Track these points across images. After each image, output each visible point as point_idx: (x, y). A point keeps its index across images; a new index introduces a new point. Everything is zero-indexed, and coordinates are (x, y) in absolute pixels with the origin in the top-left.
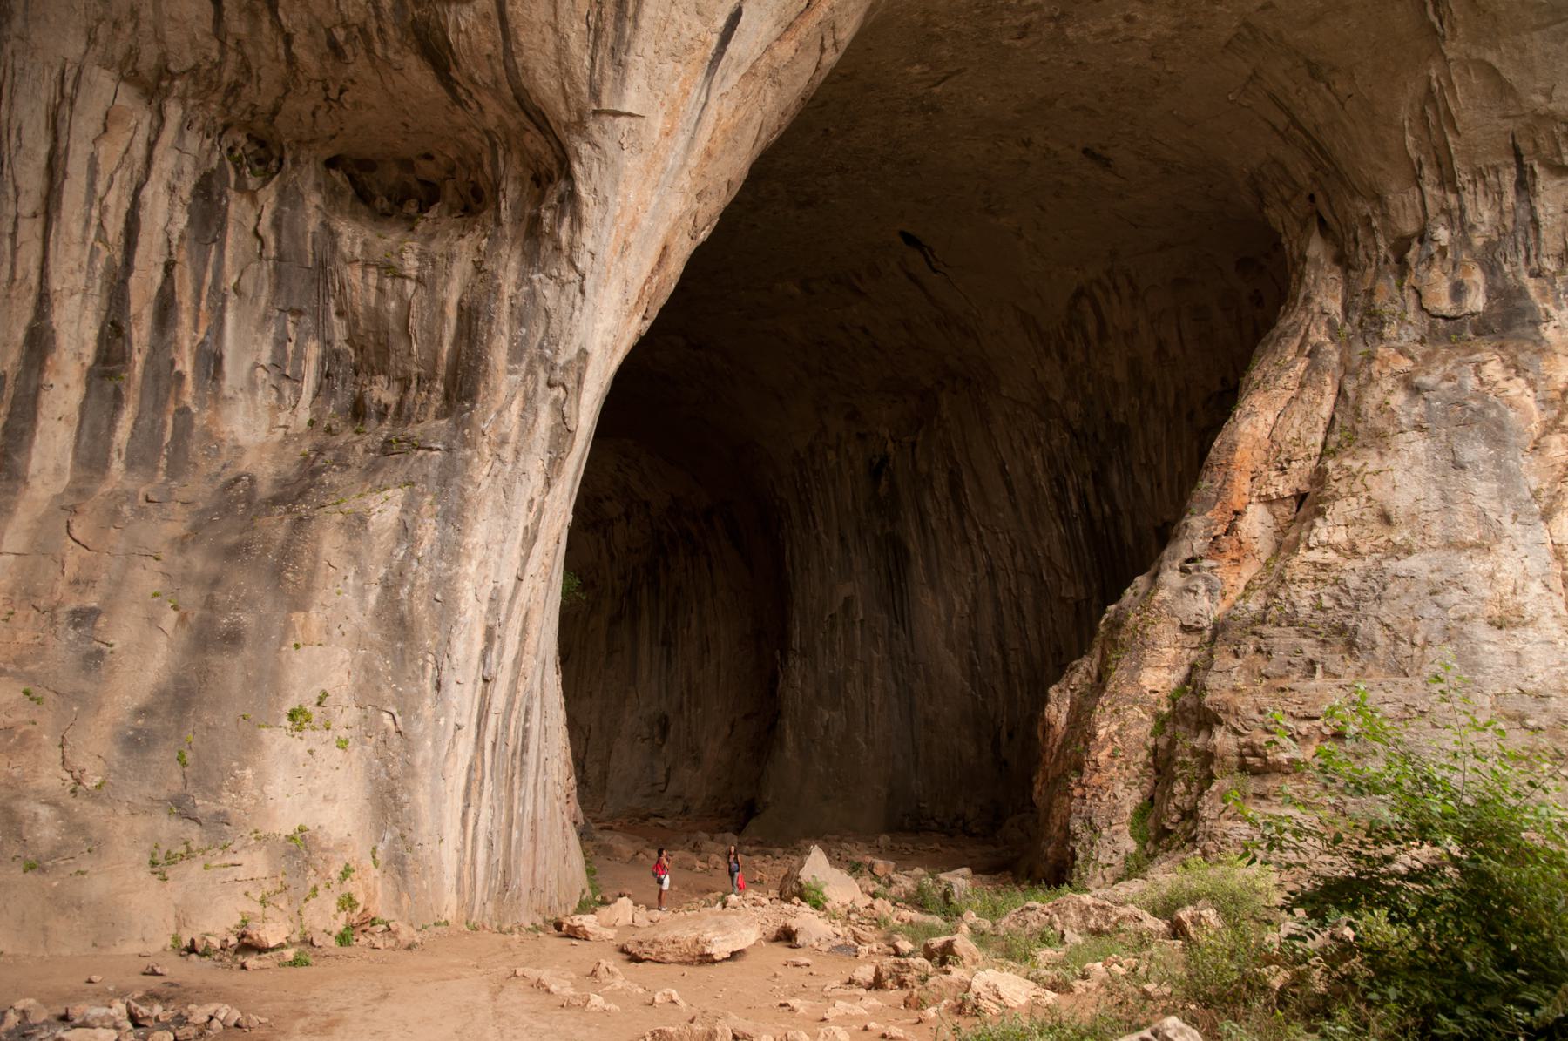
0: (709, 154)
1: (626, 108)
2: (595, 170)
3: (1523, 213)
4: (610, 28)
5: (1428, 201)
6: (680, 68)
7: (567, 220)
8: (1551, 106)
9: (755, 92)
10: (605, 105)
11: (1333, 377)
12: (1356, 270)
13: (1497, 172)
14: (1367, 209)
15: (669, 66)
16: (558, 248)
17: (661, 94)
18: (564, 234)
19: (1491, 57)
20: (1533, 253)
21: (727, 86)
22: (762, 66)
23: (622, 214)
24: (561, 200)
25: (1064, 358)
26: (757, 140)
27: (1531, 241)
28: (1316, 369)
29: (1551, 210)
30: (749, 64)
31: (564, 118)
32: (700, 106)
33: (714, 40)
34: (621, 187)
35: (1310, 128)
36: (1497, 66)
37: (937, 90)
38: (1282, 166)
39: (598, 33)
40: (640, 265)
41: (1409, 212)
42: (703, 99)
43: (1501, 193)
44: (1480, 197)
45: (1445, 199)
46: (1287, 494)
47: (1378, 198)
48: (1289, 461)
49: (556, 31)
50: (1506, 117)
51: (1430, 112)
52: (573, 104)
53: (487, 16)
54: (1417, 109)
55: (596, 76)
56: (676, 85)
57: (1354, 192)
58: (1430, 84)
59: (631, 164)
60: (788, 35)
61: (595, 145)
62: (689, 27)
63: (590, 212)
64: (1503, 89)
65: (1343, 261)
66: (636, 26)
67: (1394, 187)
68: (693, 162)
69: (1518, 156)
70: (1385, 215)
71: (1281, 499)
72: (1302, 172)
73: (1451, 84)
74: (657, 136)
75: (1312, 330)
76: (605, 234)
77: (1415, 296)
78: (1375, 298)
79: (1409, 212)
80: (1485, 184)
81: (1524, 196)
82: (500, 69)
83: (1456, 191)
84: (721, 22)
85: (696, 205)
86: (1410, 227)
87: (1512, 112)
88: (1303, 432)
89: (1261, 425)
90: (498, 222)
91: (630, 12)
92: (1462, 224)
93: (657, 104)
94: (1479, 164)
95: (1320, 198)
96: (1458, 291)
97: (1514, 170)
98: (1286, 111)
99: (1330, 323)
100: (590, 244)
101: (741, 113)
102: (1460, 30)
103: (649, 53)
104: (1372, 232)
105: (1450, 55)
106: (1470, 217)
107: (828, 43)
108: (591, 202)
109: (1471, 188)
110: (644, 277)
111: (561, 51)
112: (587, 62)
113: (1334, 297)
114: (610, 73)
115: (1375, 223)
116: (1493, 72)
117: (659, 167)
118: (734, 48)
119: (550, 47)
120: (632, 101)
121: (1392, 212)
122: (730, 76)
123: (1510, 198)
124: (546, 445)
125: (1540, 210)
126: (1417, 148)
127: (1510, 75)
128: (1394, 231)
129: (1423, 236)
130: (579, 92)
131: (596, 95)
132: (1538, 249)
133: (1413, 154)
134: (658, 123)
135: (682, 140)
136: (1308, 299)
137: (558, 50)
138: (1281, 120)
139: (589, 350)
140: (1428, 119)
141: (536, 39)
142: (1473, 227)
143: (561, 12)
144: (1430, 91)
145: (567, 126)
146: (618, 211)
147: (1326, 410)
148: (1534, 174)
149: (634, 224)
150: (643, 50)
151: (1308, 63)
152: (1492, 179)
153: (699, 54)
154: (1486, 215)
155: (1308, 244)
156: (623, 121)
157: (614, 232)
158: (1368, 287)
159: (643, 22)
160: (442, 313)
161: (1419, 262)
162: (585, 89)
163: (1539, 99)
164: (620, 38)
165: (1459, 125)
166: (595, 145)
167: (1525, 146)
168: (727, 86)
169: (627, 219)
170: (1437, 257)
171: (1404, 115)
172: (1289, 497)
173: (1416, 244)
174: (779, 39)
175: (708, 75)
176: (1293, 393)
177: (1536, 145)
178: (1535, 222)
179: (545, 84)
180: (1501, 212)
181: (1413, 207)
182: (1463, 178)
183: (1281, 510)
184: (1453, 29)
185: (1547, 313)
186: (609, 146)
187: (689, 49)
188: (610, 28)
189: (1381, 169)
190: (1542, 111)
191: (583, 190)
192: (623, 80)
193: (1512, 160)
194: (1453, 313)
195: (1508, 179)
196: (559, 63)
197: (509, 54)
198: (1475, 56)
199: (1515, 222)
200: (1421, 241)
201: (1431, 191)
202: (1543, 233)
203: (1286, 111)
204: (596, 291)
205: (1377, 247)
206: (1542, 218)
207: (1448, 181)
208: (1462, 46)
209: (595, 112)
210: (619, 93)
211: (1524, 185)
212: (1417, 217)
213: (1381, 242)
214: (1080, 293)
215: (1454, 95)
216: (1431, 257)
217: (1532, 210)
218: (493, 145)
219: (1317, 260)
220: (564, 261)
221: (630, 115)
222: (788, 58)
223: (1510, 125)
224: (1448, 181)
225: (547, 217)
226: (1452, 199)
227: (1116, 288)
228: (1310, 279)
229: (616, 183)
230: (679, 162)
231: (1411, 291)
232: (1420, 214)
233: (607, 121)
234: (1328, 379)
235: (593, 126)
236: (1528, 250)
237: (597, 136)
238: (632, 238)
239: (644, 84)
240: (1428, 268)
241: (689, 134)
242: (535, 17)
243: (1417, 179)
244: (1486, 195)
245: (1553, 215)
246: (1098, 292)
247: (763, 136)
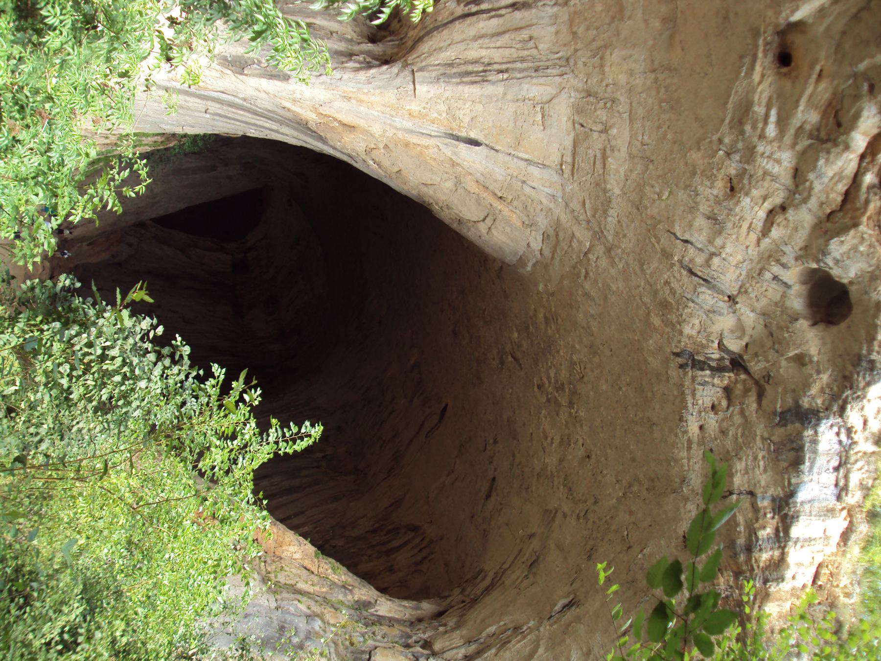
0: (407, 145)
1: (417, 87)
2: (385, 76)
4: (455, 70)
5: (455, 651)
6: (444, 115)
7: (357, 65)
9: (446, 170)
10: (416, 74)
11: (327, 593)
15: (443, 108)
16: (343, 63)
17: (428, 106)
18: (351, 64)
21: (444, 149)
22: (459, 169)
23: (364, 93)
24: (368, 63)
25: (374, 531)
26: (425, 185)
30: (459, 161)
31: (410, 58)
32: (429, 132)
33: (463, 134)
34: (378, 91)
37: (510, 359)
39: (451, 65)
40: (342, 111)
41: (447, 643)
42: (433, 134)
47: (458, 626)
49: (449, 45)
51: (509, 632)
52: (418, 59)
53: (452, 14)
55: (430, 68)
56: (435, 115)
59: (391, 96)
60: (481, 187)
61: (397, 75)
62: (464, 115)
63: (362, 75)
66: (458, 84)
68: (400, 135)
73: (524, 638)
74: (408, 107)
76: (352, 85)
79: (447, 643)
82: (432, 26)
84: (473, 135)
85: (381, 146)
86: (437, 646)
90: (359, 43)
91: (464, 80)
93: (423, 105)
100: (345, 77)
101: (434, 164)
102: (555, 626)
103: (447, 94)
107: (489, 221)
108: (367, 75)
110: (336, 116)
111: (440, 49)
112: (436, 62)
113: (390, 611)
114: (434, 74)
117: (393, 113)
118: (462, 146)
119: (442, 44)
120: (421, 89)
121: (448, 635)
122: (449, 149)
124: (234, 54)
126: (488, 636)
130: (422, 61)
131: (421, 69)
133: (484, 634)
134: (415, 107)
135: (409, 125)
137: (440, 49)
139: (290, 81)
141: (445, 37)
143: (458, 45)
145: (406, 60)
146: (366, 91)
149: (360, 101)
150: (446, 90)
151: (538, 557)
153: (454, 125)
156: (412, 87)
157: (354, 90)
159: (460, 87)
160: (309, 17)
162: (424, 64)
164: (451, 76)
165: (501, 653)
166: (397, 75)
168: (444, 149)
169: (363, 97)
171: (507, 620)
174: (477, 182)
175: (446, 134)
179: (425, 47)
181: (451, 645)
184: (556, 622)
186: (398, 81)
187: (455, 119)
188: (455, 70)
191: (373, 71)
192: (431, 83)
196: (435, 50)
197: (437, 28)
198: (541, 643)
204: (321, 83)
209: (413, 71)
210: (423, 82)
214: (415, 529)
215: (519, 642)
218: (401, 39)
220: (337, 65)
221: (415, 89)
222: (469, 188)
225: (361, 58)
227: (421, 551)
228: (405, 603)
229: (379, 87)
230: (399, 125)
233: (410, 78)
234: (324, 590)
235: (407, 72)
237: (402, 75)
238: (354, 101)
239: (431, 95)
241: (413, 128)
242: (455, 34)
246: (417, 540)
247: (431, 192)
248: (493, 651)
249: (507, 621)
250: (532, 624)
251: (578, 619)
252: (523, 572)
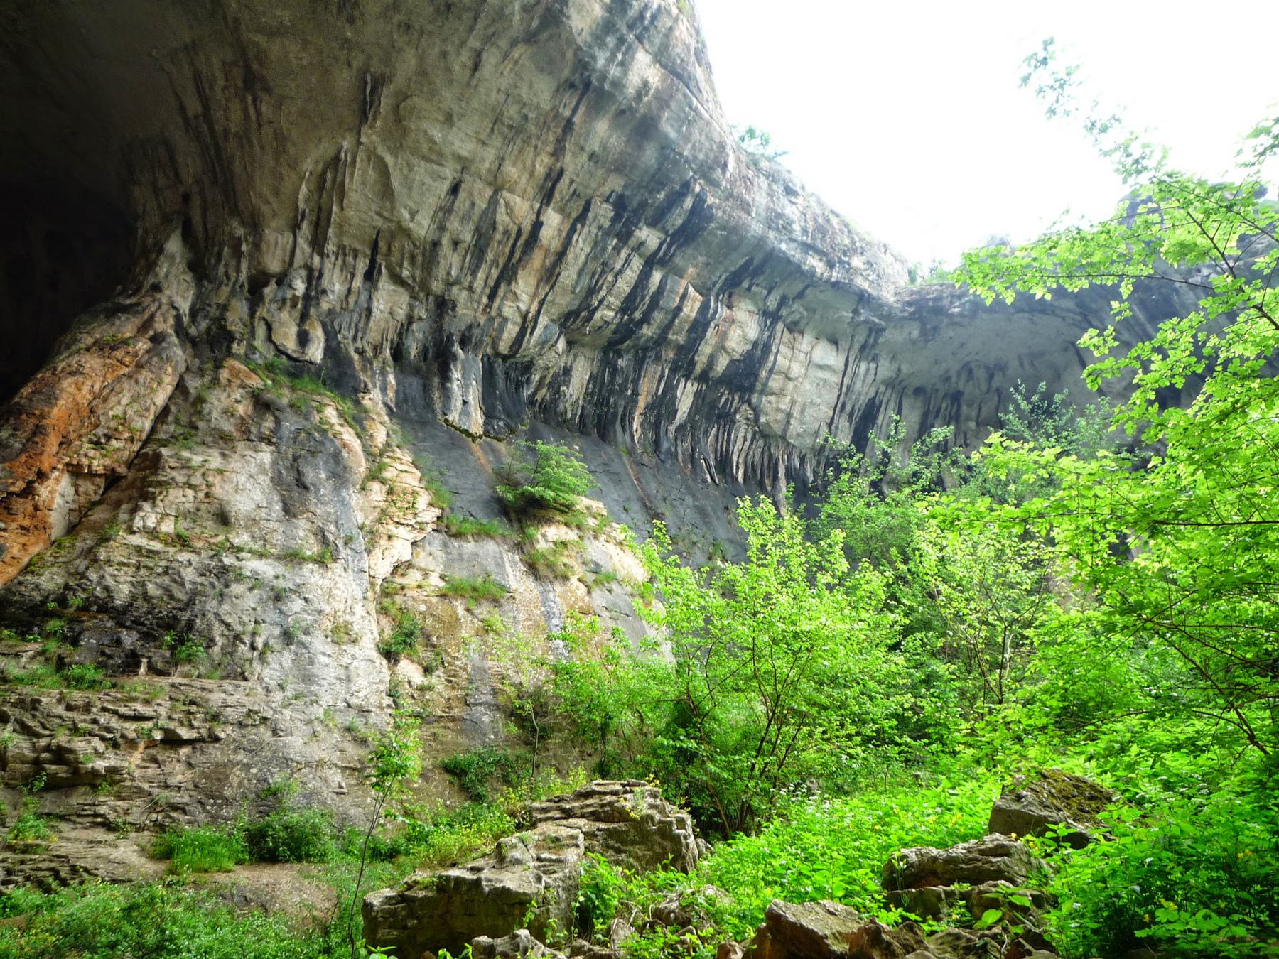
3: (363, 298)
5: (298, 252)
8: (411, 225)
11: (175, 369)
12: (210, 282)
13: (355, 257)
14: (240, 232)
19: (389, 159)
20: (360, 335)
27: (361, 325)
28: (159, 355)
29: (382, 307)
35: (218, 128)
36: (391, 170)
38: (171, 153)
41: (279, 252)
43: (353, 275)
44: (337, 271)
45: (311, 257)
46: (100, 470)
48: (108, 438)
50: (378, 214)
51: (329, 176)
54: (320, 167)
57: (235, 212)
58: (339, 152)
64: (386, 192)
65: (199, 269)
67: (273, 224)
69: (375, 248)
70: (257, 246)
71: (92, 475)
72: (191, 166)
73: (354, 162)
75: (158, 318)
77: (265, 327)
78: (228, 314)
79: (279, 252)
80: (344, 262)
81: (368, 284)
83: (322, 254)
87: (386, 214)
88: (130, 412)
89: (85, 390)
92: (318, 285)
94: (346, 242)
95: (196, 201)
96: (303, 339)
97: (368, 261)
98: (205, 103)
99: (178, 318)
102: (378, 123)
104: (237, 254)
105: (363, 139)
106: (325, 283)
109: (333, 258)
115: (244, 248)
116: (384, 172)
123: (358, 282)
125: (375, 304)
126: (307, 200)
127: (396, 183)
128: (259, 263)
129: (282, 279)
132: (364, 333)
133: (301, 205)
136: (157, 288)
138: (194, 106)
140: (325, 181)
142: (324, 292)
144: (337, 158)
147: (161, 398)
148: (380, 272)
152: (350, 259)
154: (337, 287)
155: (168, 238)
158: (221, 301)
161: (273, 301)
163: (406, 214)
165: (345, 201)
167: (382, 245)
170: (289, 303)
172: (100, 476)
173: (273, 282)
176: (126, 370)
177: (389, 249)
178: (369, 311)
180: (349, 290)
181: (284, 250)
182: (330, 247)
183: (87, 487)
184: (375, 119)
185: (366, 386)
189: (268, 203)
190: (405, 224)
193: (368, 252)
194: (295, 355)
195: (362, 266)
198: (379, 151)
199: (356, 303)
200: (279, 283)
201: (303, 245)
202: (372, 323)
203: (205, 103)
205: (238, 271)
206: (374, 310)
207: (318, 243)
208: (374, 137)
211: (371, 276)
212: (284, 261)
213: (244, 266)
216: (284, 301)
217: (370, 299)
219: (172, 257)
223: (379, 223)
224: (318, 243)
226: (317, 259)
231: (262, 323)
232: (287, 259)
234: (170, 370)
236: (357, 332)
240: (280, 309)
243: (295, 227)
244: (342, 270)
245: (382, 312)
248: (335, 208)
249: (310, 168)
250: (346, 145)
251: (403, 96)
252: (243, 101)
